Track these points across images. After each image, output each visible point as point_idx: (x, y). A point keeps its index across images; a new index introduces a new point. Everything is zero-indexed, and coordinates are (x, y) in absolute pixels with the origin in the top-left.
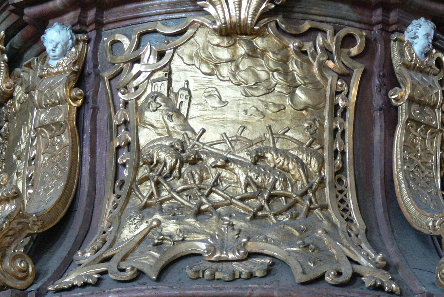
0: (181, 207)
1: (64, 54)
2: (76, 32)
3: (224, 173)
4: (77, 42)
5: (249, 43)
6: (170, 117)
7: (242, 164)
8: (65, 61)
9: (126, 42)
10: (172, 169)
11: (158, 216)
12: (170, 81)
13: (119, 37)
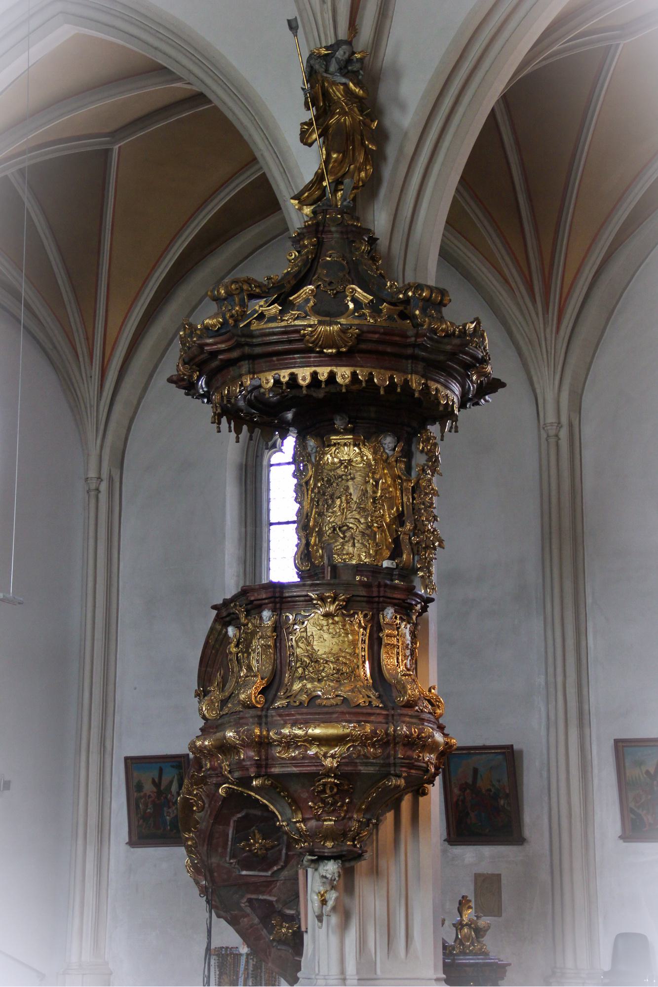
0: (313, 678)
1: (269, 620)
2: (273, 611)
3: (326, 665)
4: (273, 615)
5: (333, 619)
6: (307, 646)
7: (332, 662)
8: (270, 623)
9: (291, 617)
10: (309, 664)
11: (305, 681)
12: (307, 632)
13: (287, 614)
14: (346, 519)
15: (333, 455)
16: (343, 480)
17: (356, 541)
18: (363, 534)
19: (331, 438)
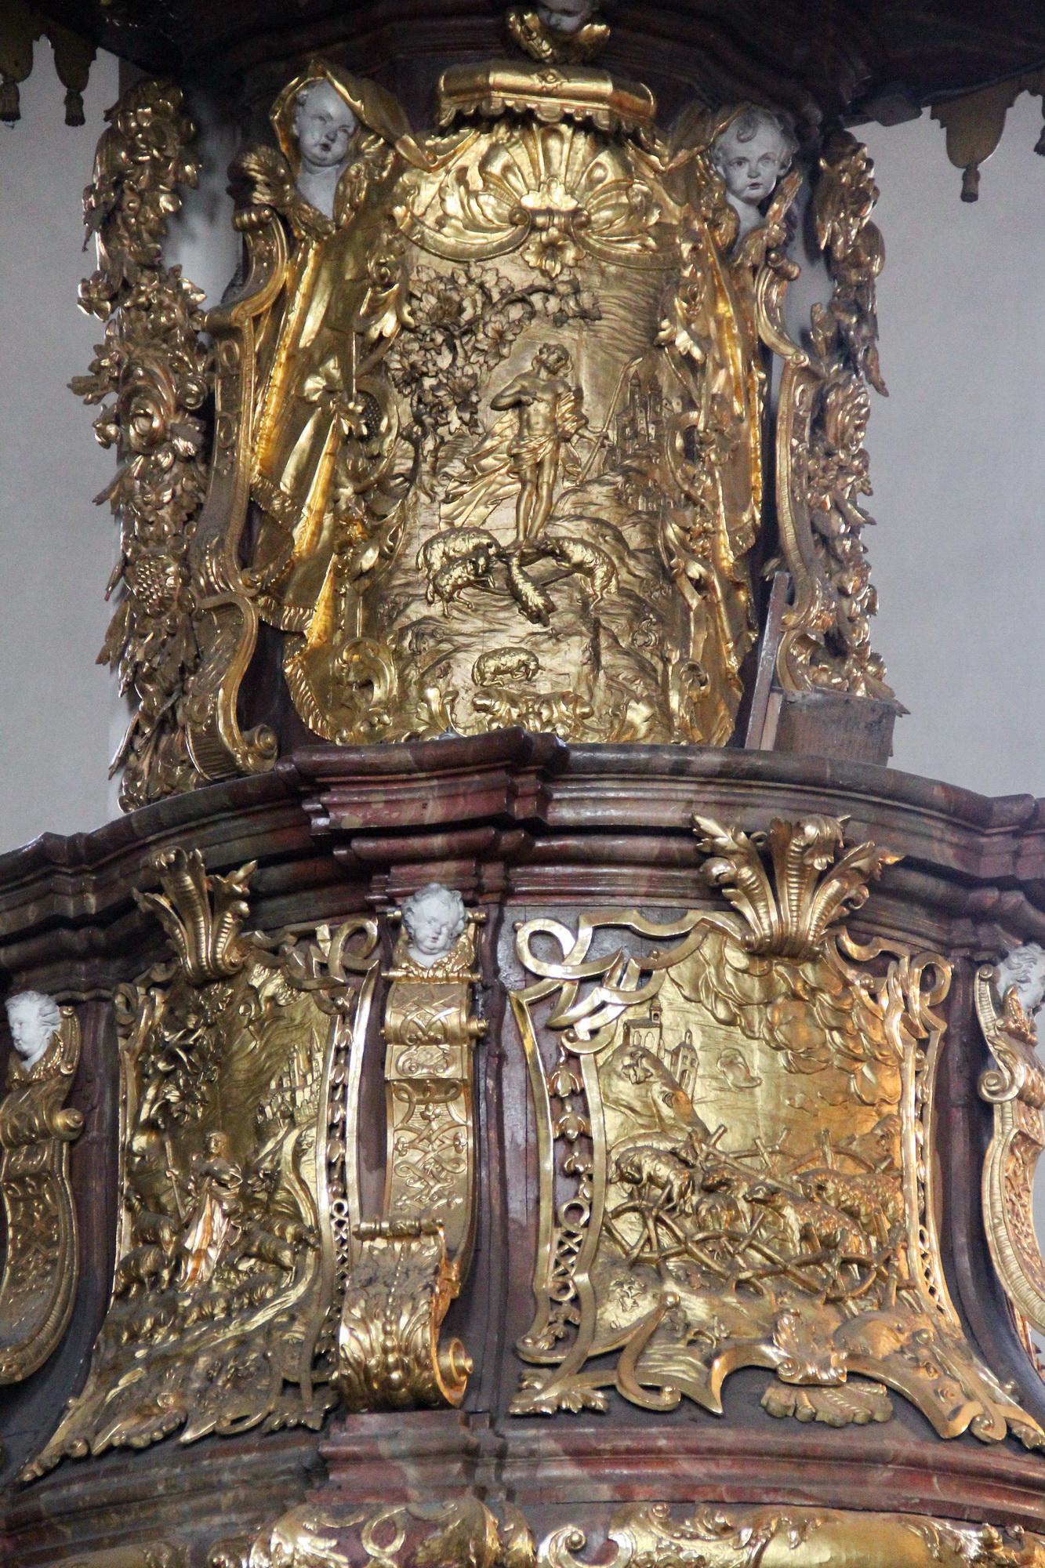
2: (469, 904)
14: (550, 518)
15: (475, 179)
16: (533, 314)
17: (604, 642)
18: (639, 609)
19: (497, 78)
